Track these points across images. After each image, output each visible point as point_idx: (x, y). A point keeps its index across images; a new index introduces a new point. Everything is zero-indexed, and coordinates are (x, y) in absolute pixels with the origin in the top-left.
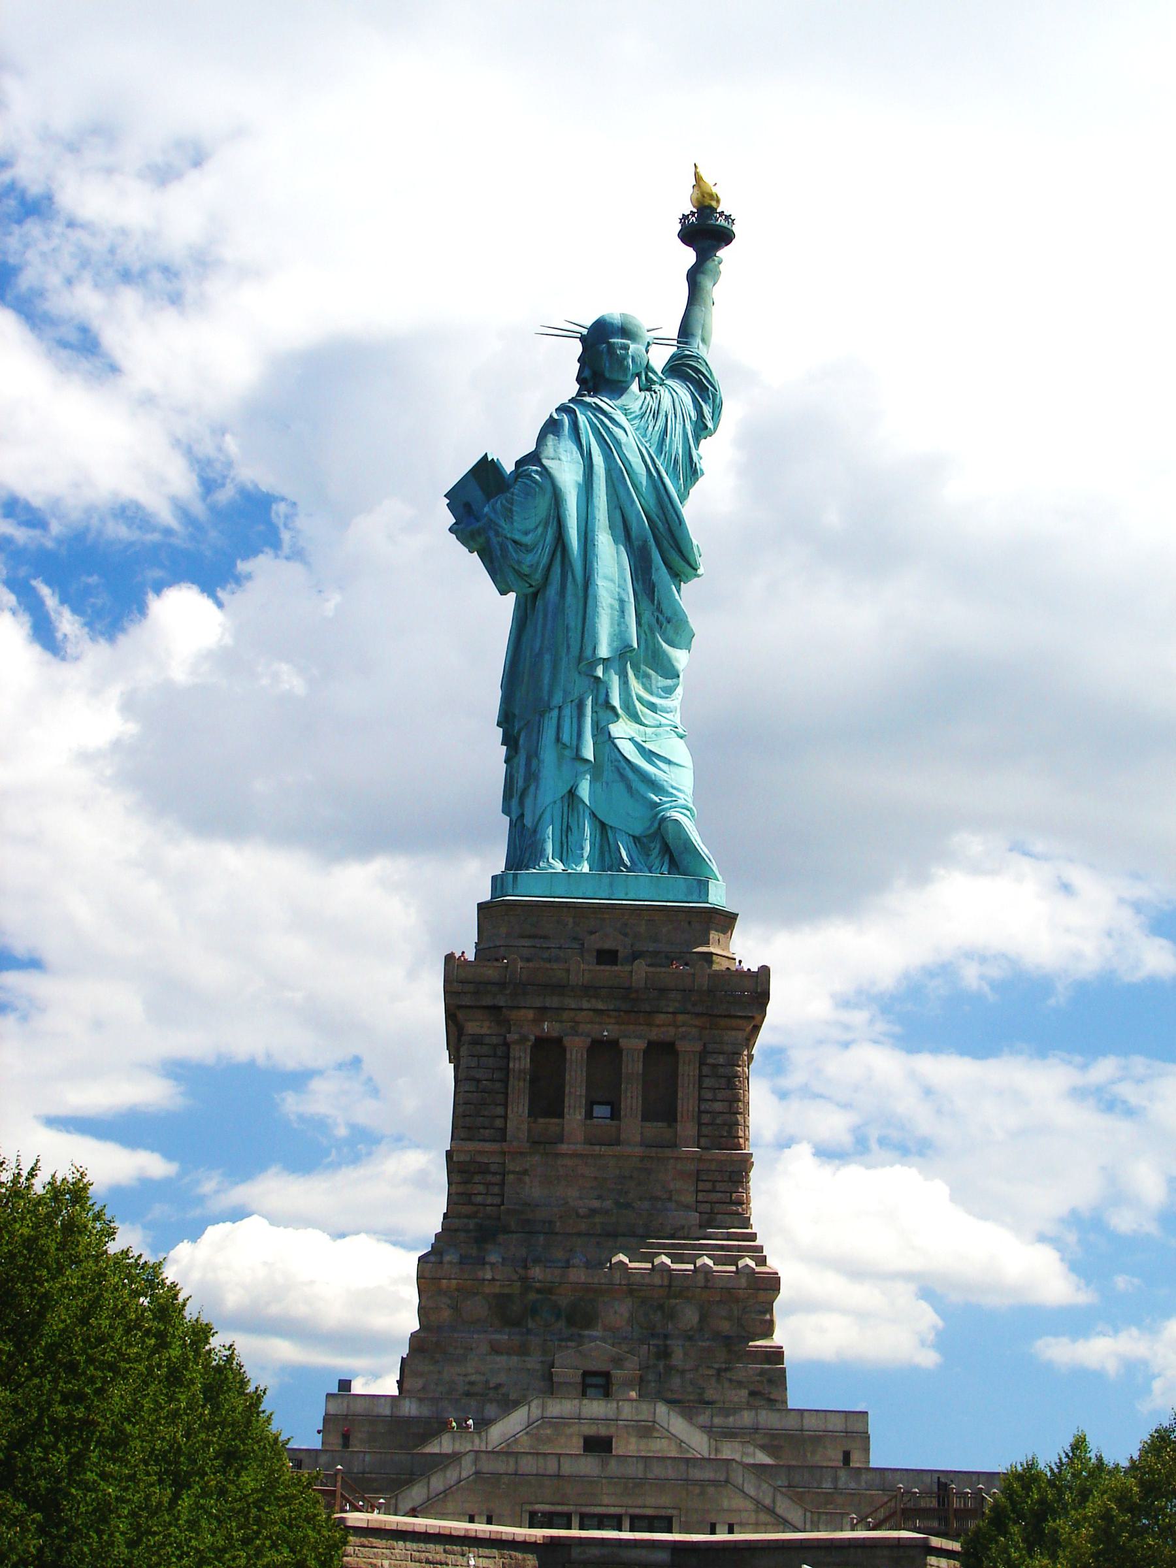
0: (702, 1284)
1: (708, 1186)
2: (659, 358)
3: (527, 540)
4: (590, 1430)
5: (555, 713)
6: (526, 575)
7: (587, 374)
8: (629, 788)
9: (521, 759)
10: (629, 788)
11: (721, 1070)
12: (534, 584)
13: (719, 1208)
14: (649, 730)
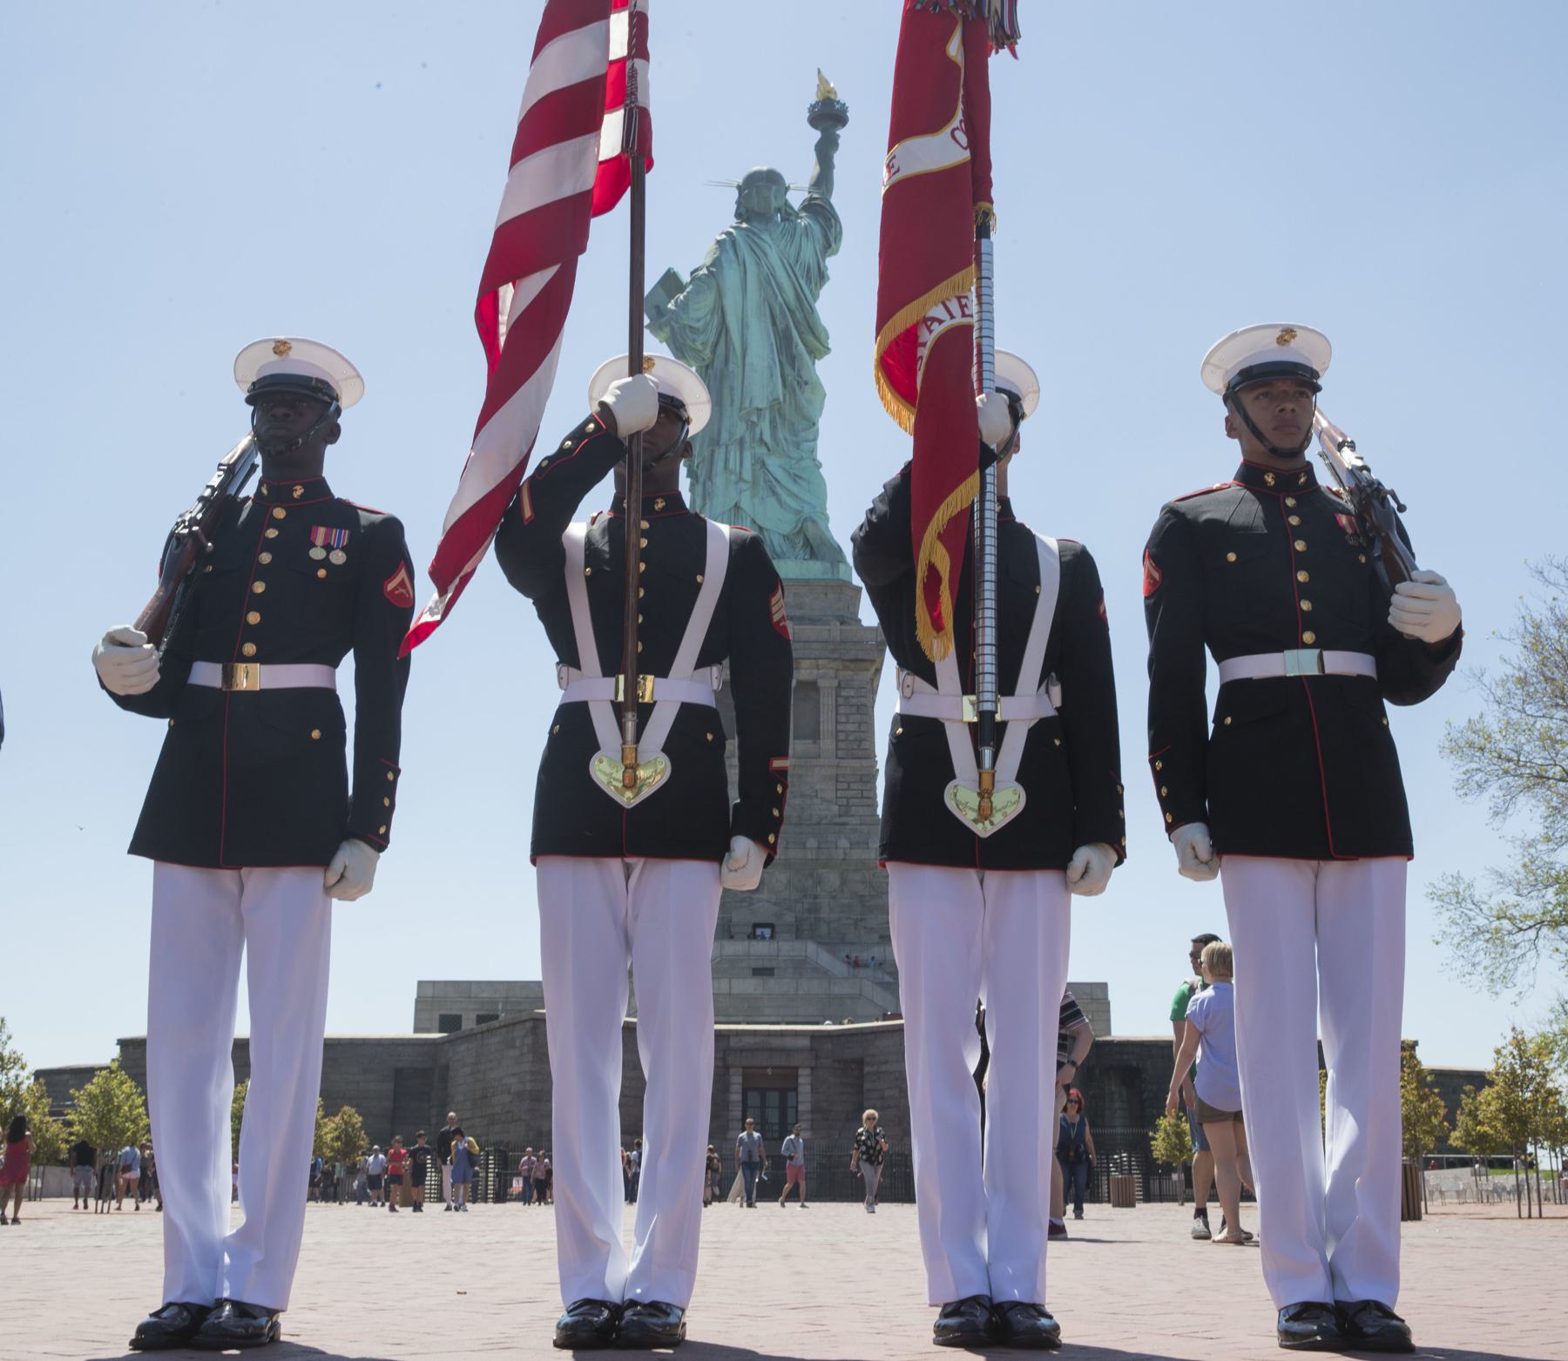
0: (842, 857)
1: (845, 786)
2: (796, 199)
3: (699, 325)
4: (759, 964)
5: (723, 450)
6: (699, 351)
7: (743, 210)
8: (780, 501)
9: (699, 488)
10: (780, 501)
11: (853, 701)
12: (706, 358)
13: (852, 801)
14: (794, 462)
